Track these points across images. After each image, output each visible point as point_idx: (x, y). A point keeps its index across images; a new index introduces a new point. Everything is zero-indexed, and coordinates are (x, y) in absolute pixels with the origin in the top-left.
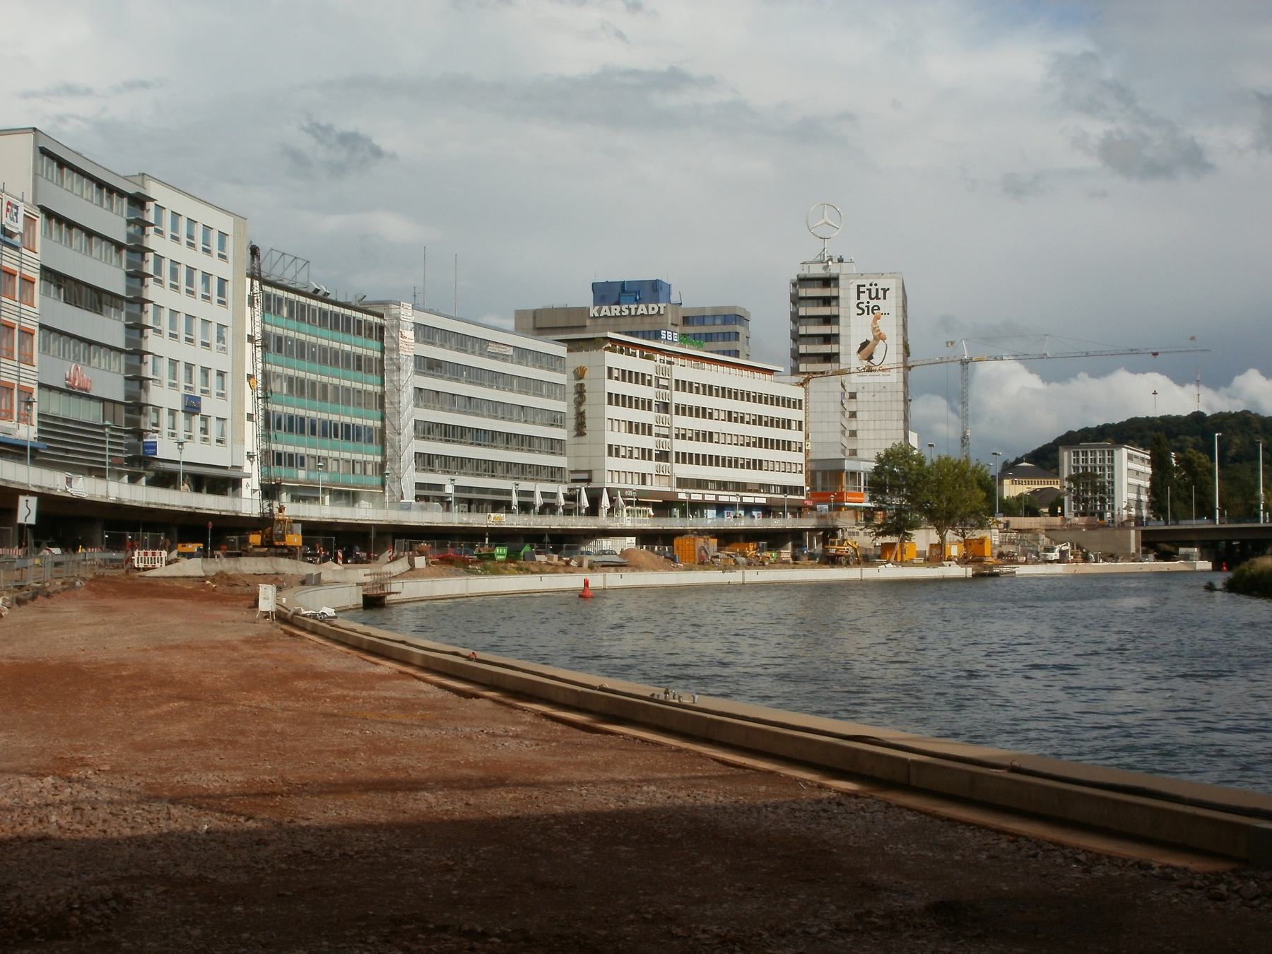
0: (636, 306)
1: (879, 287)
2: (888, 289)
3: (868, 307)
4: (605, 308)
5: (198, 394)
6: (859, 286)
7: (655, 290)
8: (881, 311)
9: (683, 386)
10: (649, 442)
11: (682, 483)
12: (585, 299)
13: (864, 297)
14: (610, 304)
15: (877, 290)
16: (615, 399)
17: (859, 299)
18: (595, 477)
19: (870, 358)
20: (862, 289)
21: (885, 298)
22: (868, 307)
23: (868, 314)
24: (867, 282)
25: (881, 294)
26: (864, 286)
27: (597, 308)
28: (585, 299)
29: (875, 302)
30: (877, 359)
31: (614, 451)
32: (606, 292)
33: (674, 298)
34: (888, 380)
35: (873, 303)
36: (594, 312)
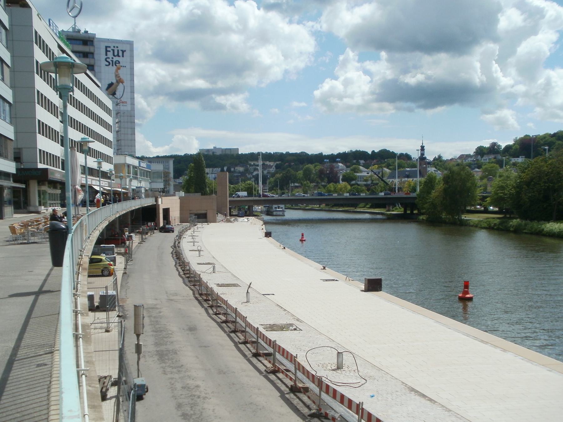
2: (125, 51)
3: (112, 61)
6: (106, 47)
8: (121, 64)
15: (118, 51)
17: (106, 55)
19: (114, 94)
20: (108, 49)
21: (123, 56)
22: (112, 61)
24: (112, 45)
25: (121, 54)
26: (110, 47)
29: (116, 59)
30: (118, 94)
35: (116, 59)
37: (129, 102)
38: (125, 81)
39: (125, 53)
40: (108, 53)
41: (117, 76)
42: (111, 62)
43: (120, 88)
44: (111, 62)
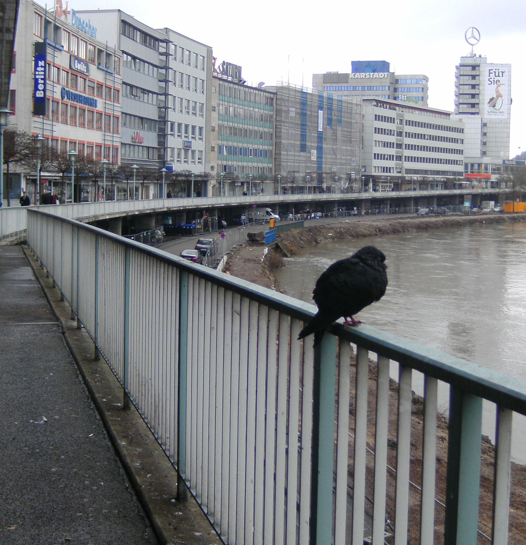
0: (373, 73)
1: (500, 71)
3: (494, 81)
4: (358, 74)
5: (190, 139)
6: (490, 70)
7: (383, 66)
8: (500, 83)
9: (410, 123)
10: (392, 151)
11: (408, 171)
12: (347, 69)
13: (492, 76)
14: (360, 72)
15: (499, 72)
16: (378, 131)
17: (489, 76)
18: (368, 169)
19: (494, 106)
20: (491, 72)
21: (502, 76)
22: (494, 81)
23: (494, 84)
25: (501, 74)
26: (492, 70)
27: (354, 74)
28: (347, 69)
29: (498, 78)
30: (498, 106)
31: (377, 156)
32: (358, 66)
33: (391, 70)
34: (503, 117)
36: (351, 76)
37: (506, 112)
38: (503, 96)
39: (504, 73)
40: (491, 74)
41: (497, 92)
42: (493, 82)
43: (499, 101)
44: (493, 82)
